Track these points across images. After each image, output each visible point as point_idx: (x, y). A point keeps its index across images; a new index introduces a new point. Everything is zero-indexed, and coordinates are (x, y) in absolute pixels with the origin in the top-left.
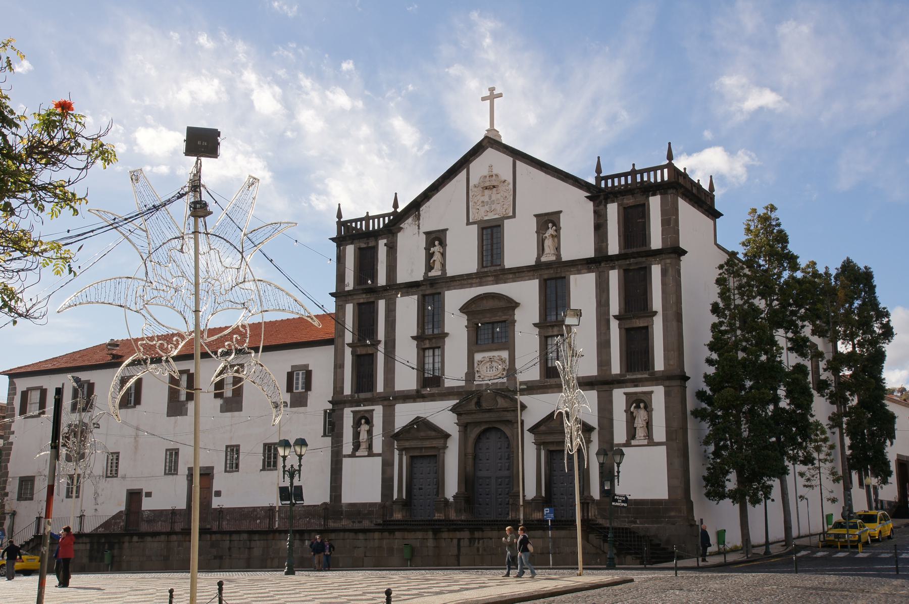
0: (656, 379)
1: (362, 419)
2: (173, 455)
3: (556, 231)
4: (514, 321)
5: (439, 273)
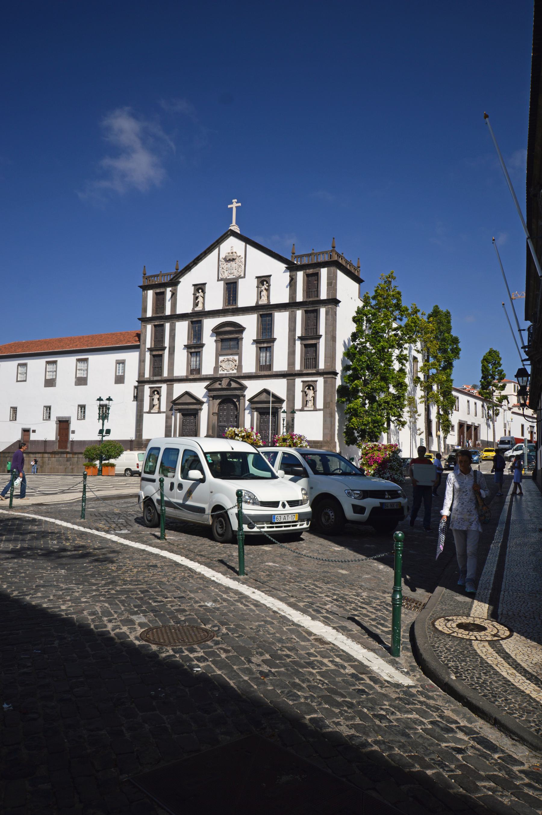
1: (156, 391)
2: (48, 408)
3: (268, 286)
4: (242, 339)
5: (201, 309)
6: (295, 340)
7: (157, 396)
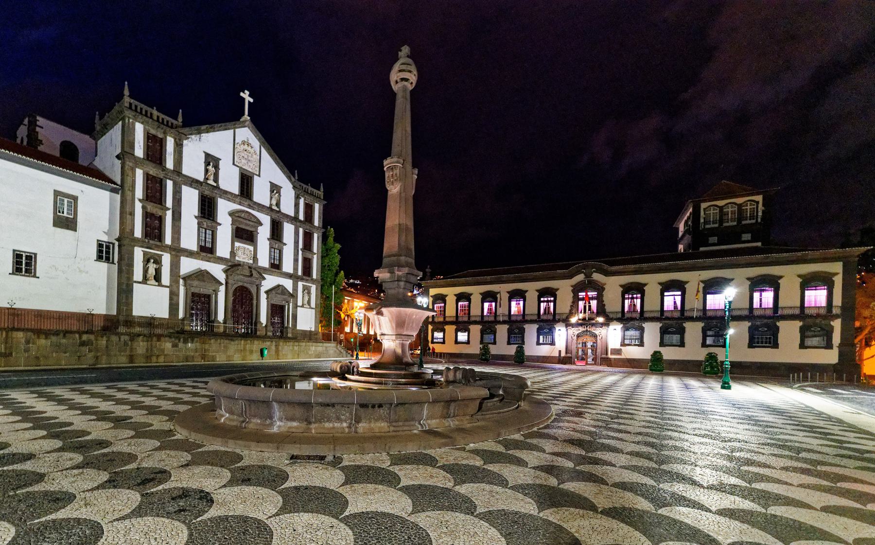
0: (313, 281)
6: (298, 251)
7: (155, 266)
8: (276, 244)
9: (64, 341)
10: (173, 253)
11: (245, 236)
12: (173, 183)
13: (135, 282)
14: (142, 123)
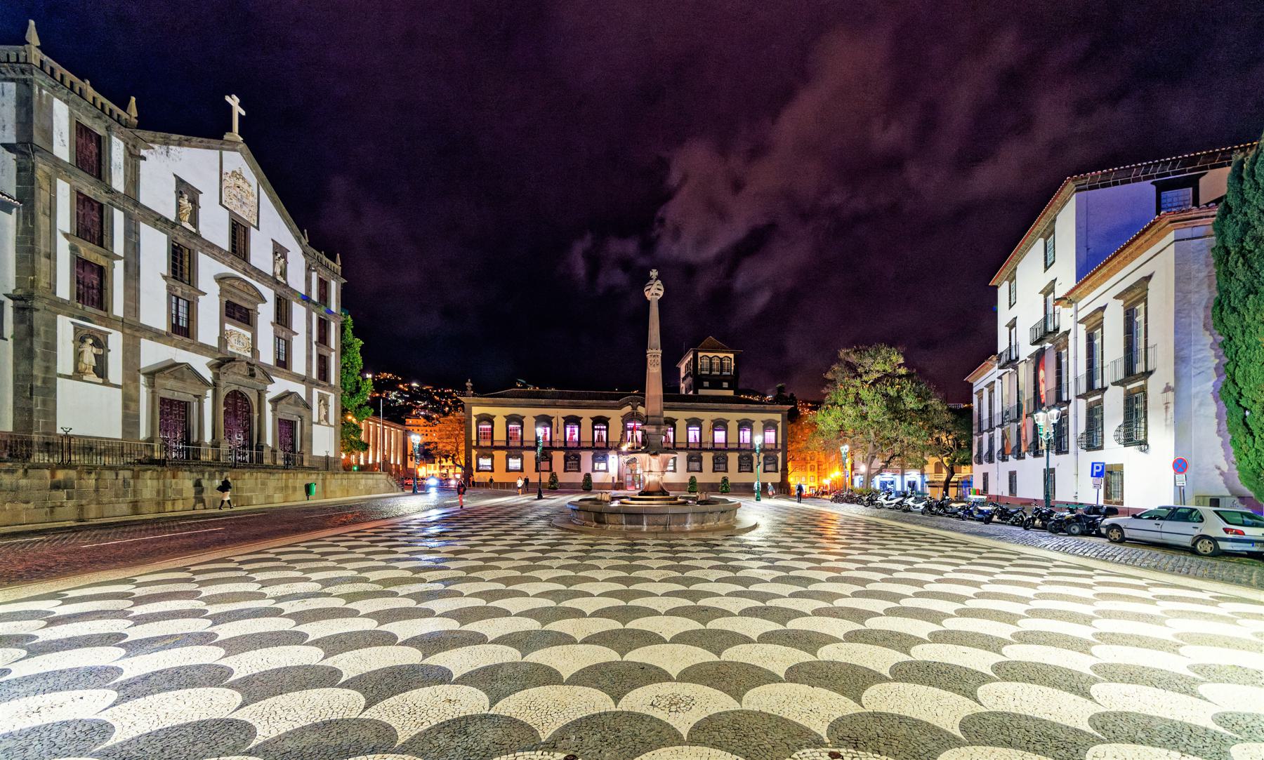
6: (311, 343)
7: (95, 350)
8: (283, 331)
9: (23, 482)
10: (127, 331)
11: (237, 315)
12: (125, 216)
13: (61, 376)
14: (67, 102)
